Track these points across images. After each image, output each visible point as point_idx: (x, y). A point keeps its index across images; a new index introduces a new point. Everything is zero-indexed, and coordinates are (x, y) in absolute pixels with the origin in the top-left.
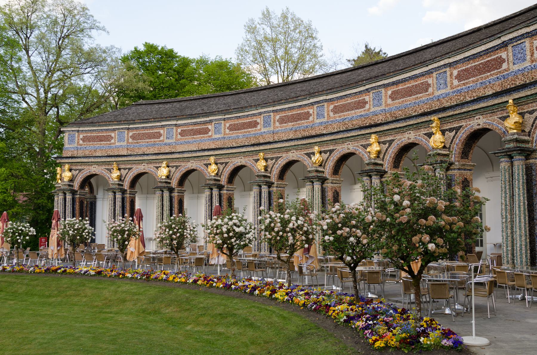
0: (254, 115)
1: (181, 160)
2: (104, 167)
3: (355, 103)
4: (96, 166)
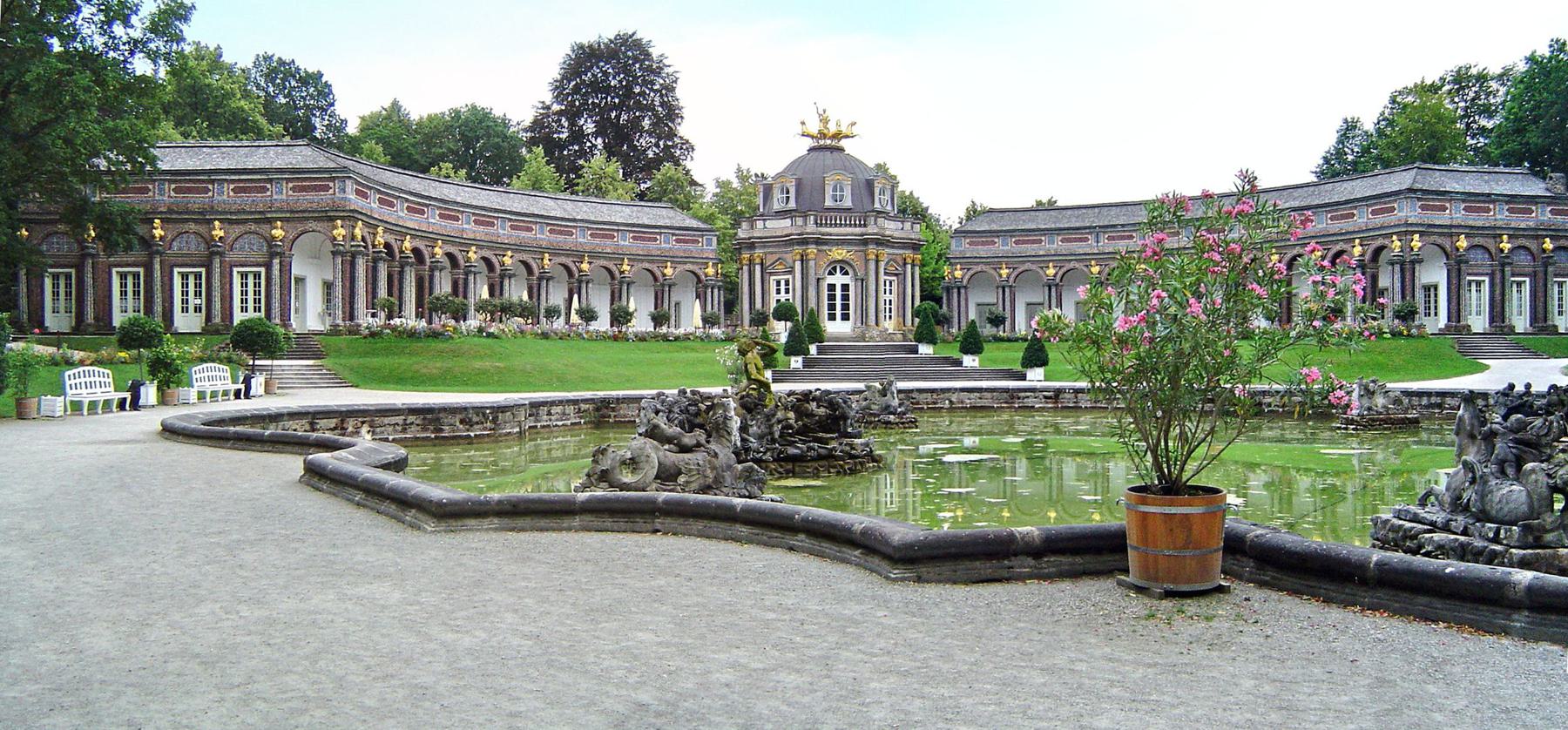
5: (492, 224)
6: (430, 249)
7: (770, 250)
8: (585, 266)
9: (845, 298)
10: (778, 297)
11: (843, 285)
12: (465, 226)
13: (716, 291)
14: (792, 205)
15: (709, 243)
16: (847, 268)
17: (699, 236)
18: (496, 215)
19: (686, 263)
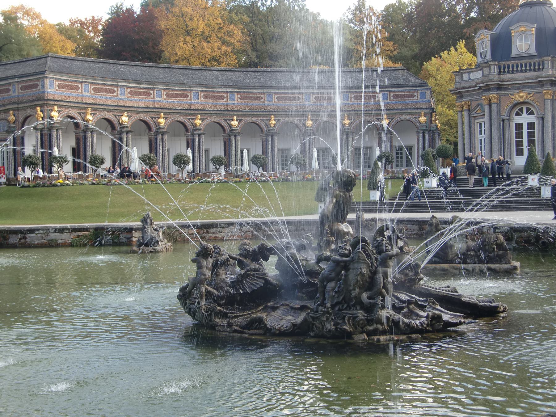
0: (186, 90)
1: (133, 112)
2: (75, 111)
3: (254, 97)
4: (71, 109)
5: (223, 98)
6: (155, 120)
7: (475, 97)
8: (309, 123)
9: (531, 135)
10: (480, 137)
11: (528, 124)
12: (193, 101)
13: (427, 136)
14: (489, 57)
15: (423, 95)
16: (532, 109)
17: (414, 91)
18: (224, 90)
19: (401, 114)
